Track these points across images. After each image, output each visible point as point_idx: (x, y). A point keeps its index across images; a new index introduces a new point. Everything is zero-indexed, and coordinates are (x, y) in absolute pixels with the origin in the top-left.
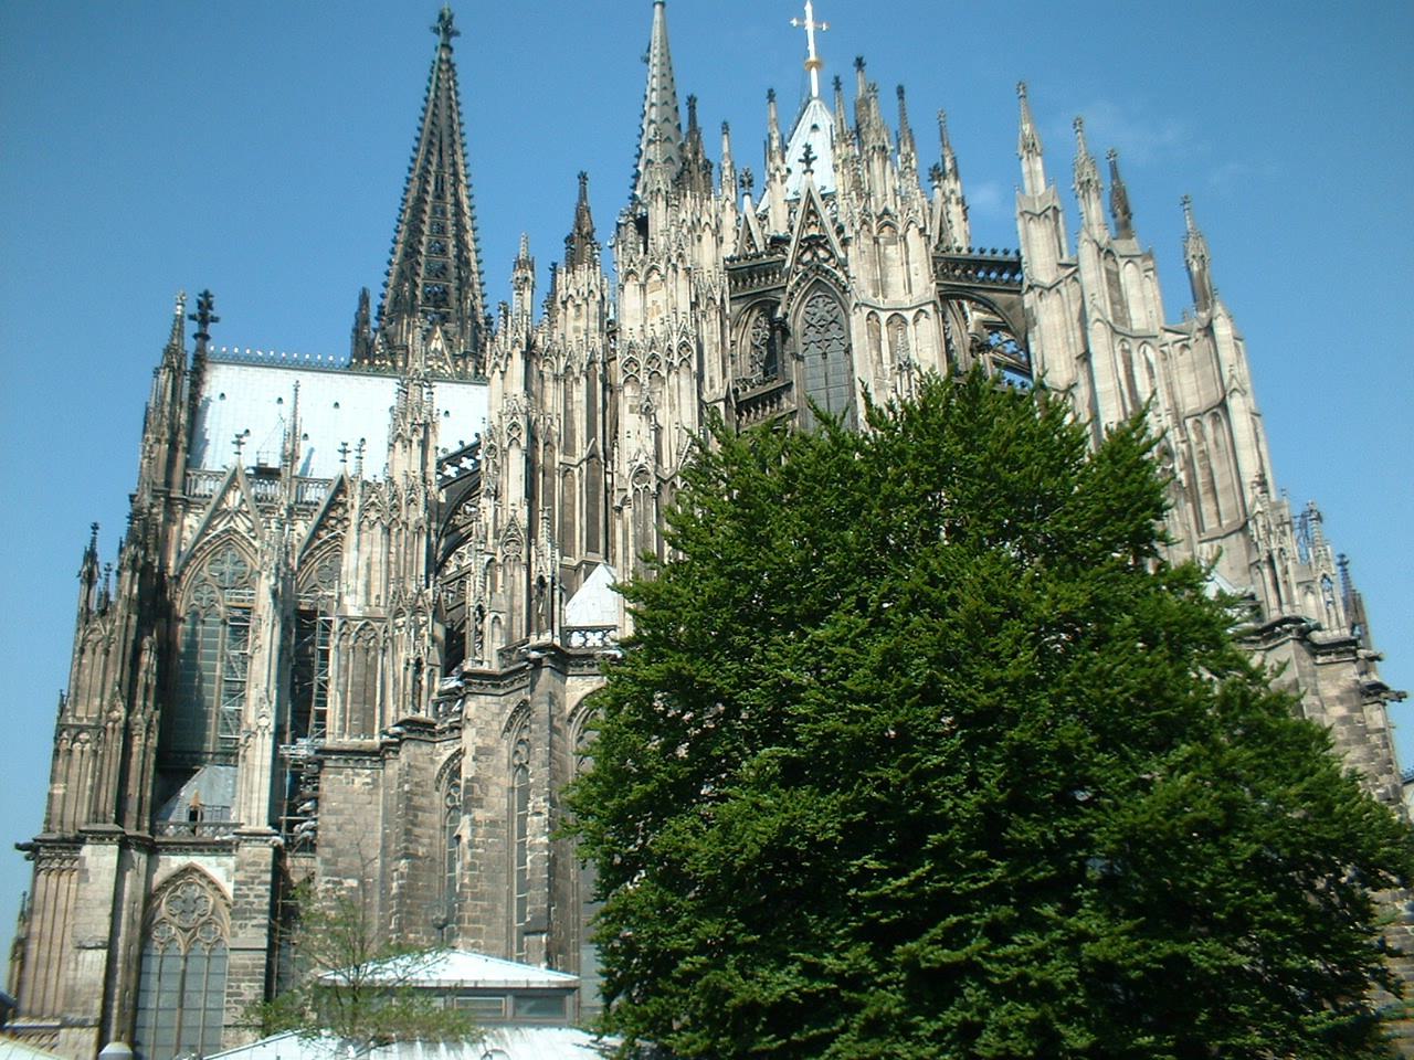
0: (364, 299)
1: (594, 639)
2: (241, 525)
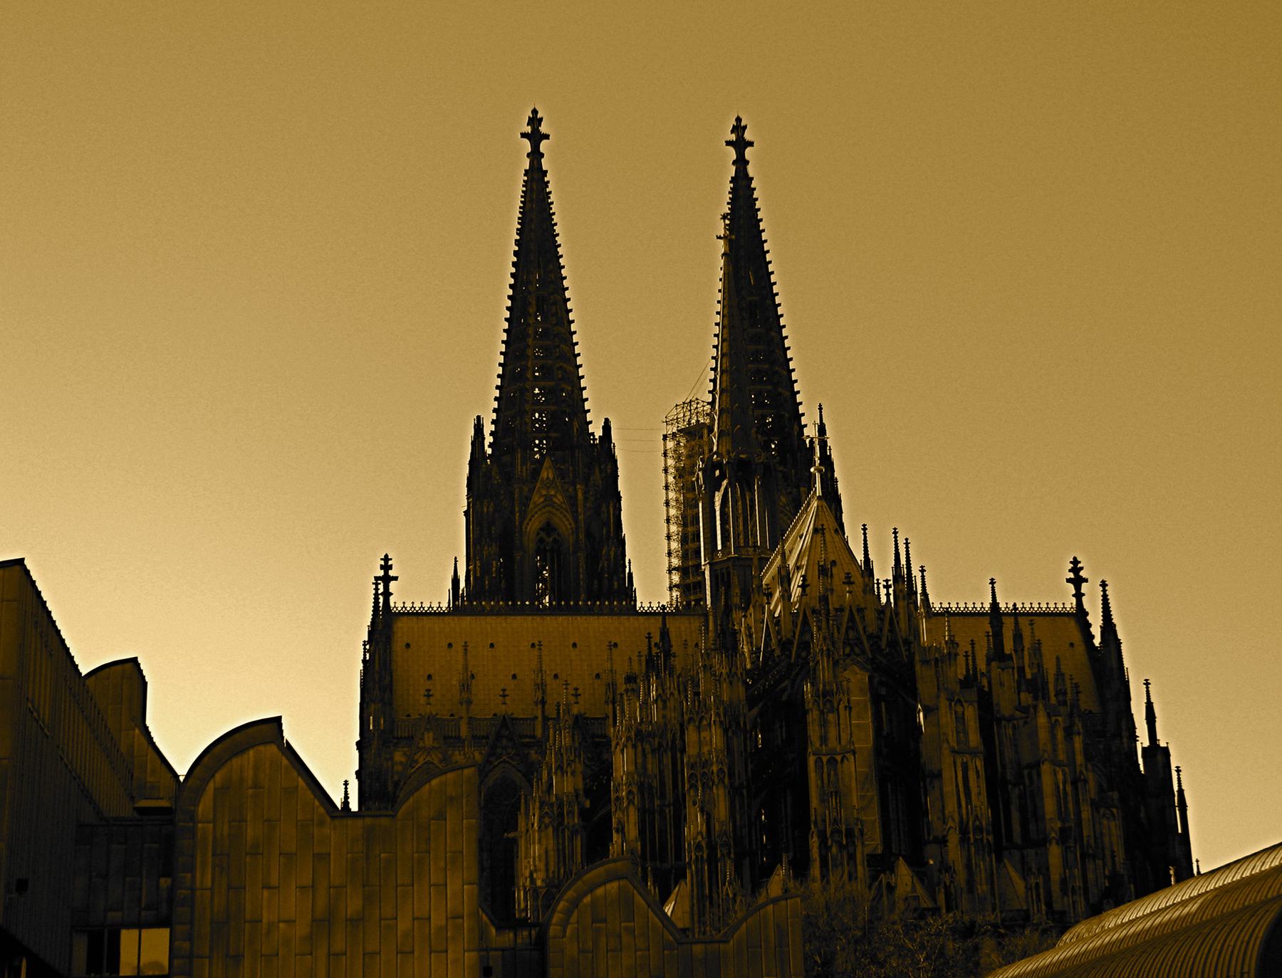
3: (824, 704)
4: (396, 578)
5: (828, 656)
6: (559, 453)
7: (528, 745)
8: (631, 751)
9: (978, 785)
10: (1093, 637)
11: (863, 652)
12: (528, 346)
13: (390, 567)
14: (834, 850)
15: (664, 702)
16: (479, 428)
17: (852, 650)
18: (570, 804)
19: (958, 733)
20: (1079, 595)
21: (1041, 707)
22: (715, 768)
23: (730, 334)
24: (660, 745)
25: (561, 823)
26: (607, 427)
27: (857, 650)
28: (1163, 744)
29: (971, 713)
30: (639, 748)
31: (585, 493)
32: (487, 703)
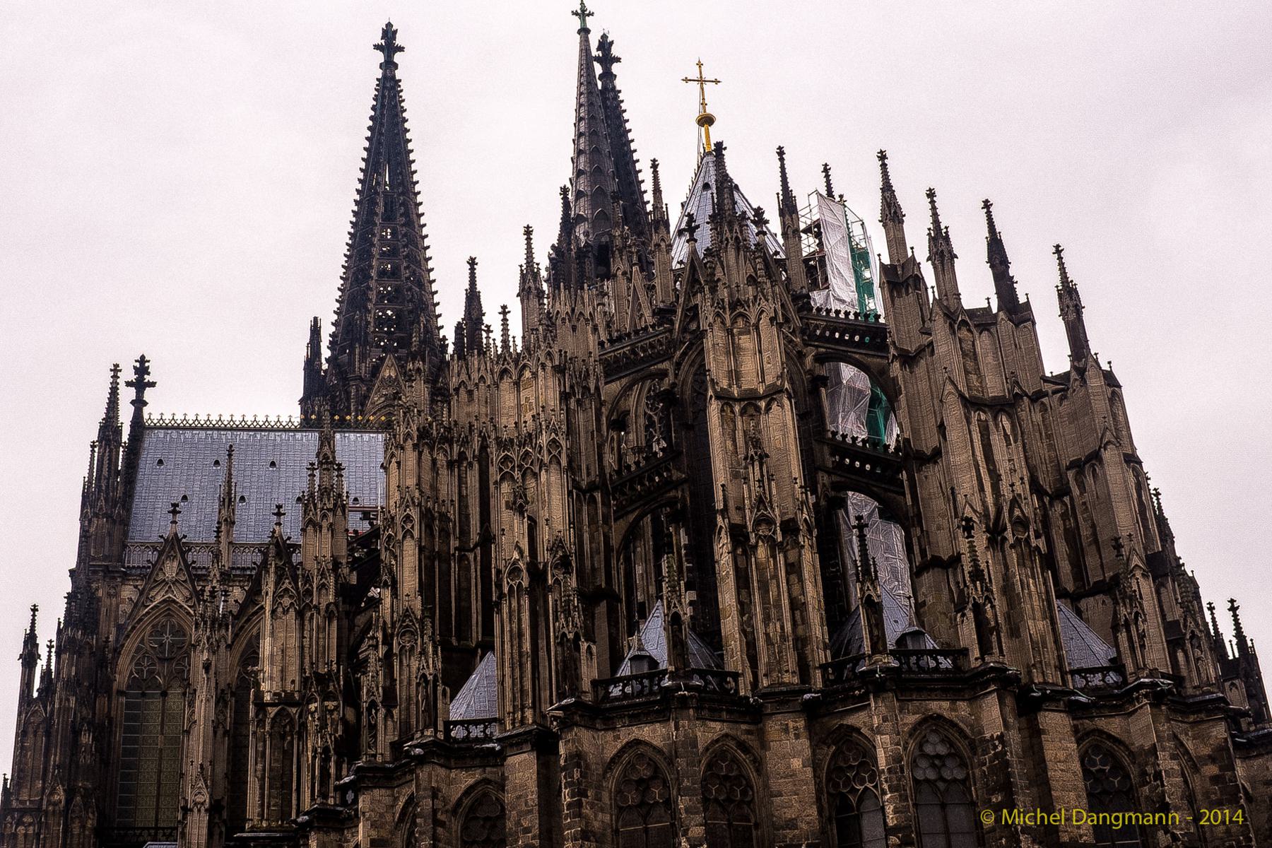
0: (315, 330)
1: (476, 732)
2: (179, 596)
3: (734, 322)
14: (762, 552)
15: (470, 393)
19: (967, 373)
24: (462, 456)
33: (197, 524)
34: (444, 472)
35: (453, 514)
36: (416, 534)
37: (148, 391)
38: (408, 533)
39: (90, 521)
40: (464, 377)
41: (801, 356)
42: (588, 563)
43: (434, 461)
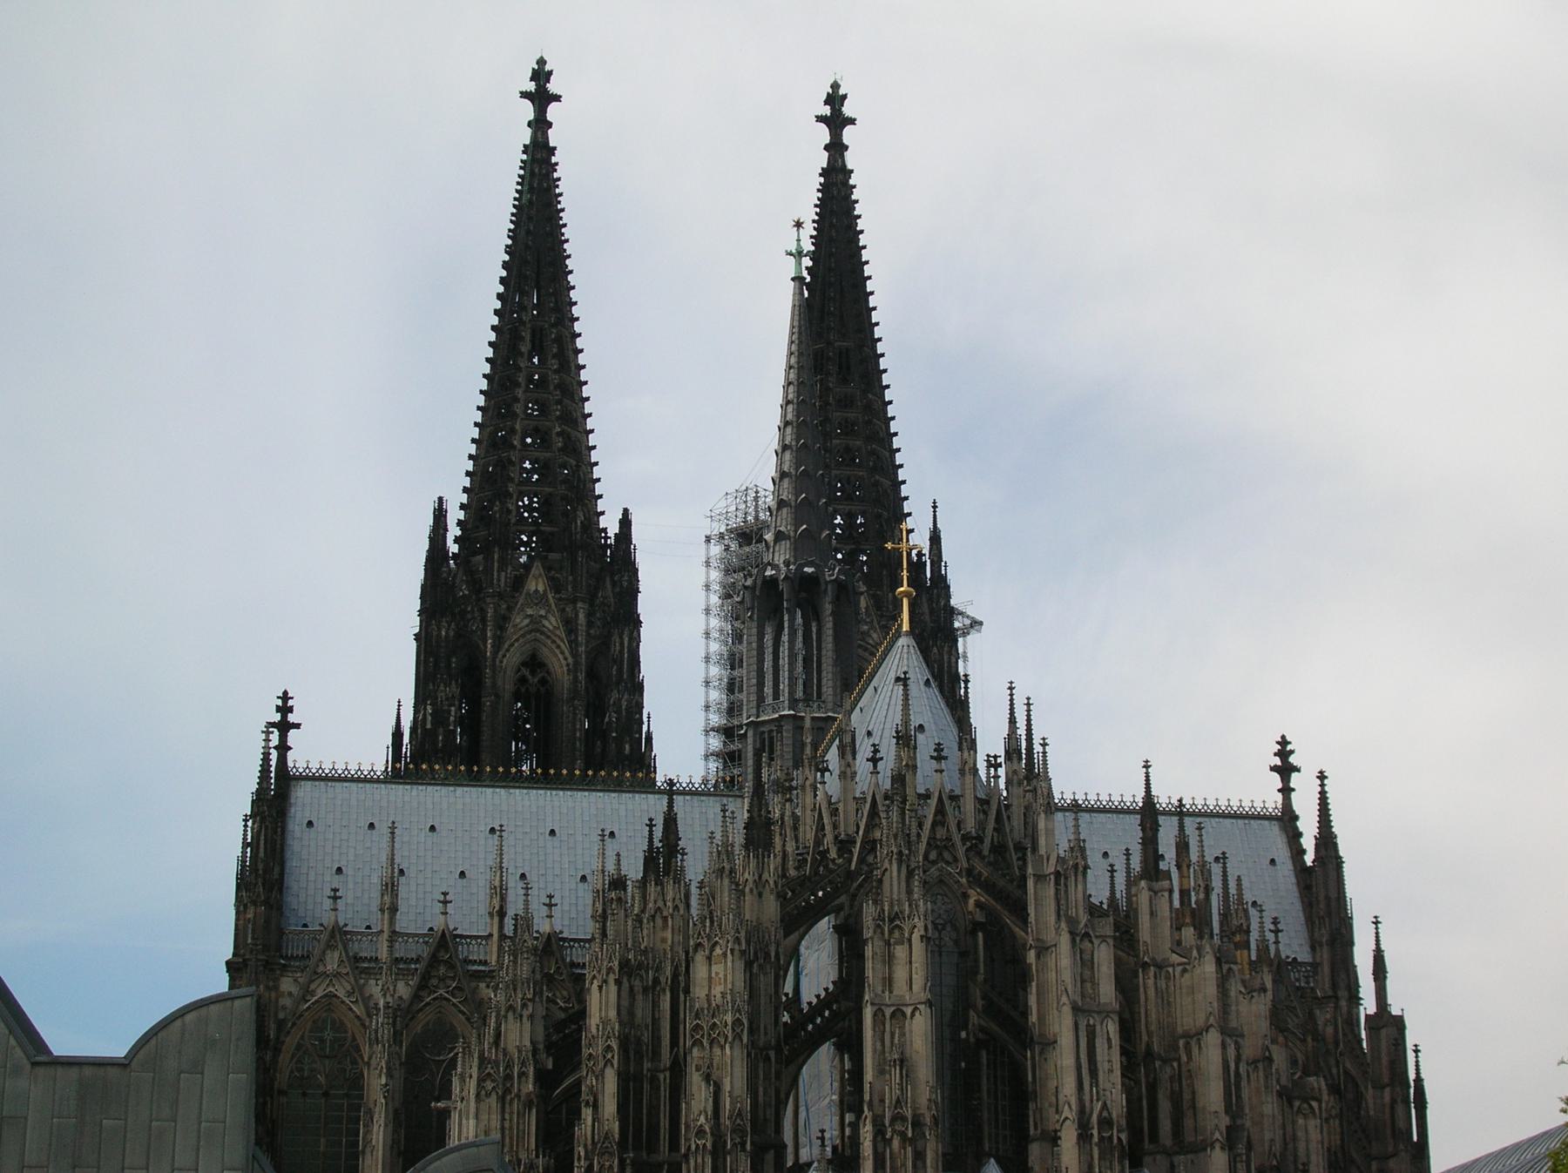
3: (891, 932)
4: (297, 726)
5: (900, 862)
6: (553, 556)
7: (478, 976)
8: (613, 988)
9: (1110, 1058)
10: (1304, 852)
11: (956, 860)
12: (516, 400)
13: (291, 710)
14: (896, 1143)
15: (665, 919)
16: (440, 514)
17: (940, 854)
18: (523, 1064)
19: (1083, 981)
20: (1286, 791)
21: (1208, 948)
22: (729, 1018)
23: (799, 394)
24: (656, 981)
25: (507, 1091)
26: (626, 522)
27: (946, 855)
28: (1395, 1011)
29: (1104, 956)
30: (626, 985)
31: (589, 615)
32: (419, 913)
33: (360, 906)
34: (640, 997)
35: (646, 1037)
36: (615, 1062)
37: (292, 733)
38: (608, 1062)
39: (245, 906)
40: (660, 904)
41: (965, 896)
42: (761, 1113)
43: (631, 988)
